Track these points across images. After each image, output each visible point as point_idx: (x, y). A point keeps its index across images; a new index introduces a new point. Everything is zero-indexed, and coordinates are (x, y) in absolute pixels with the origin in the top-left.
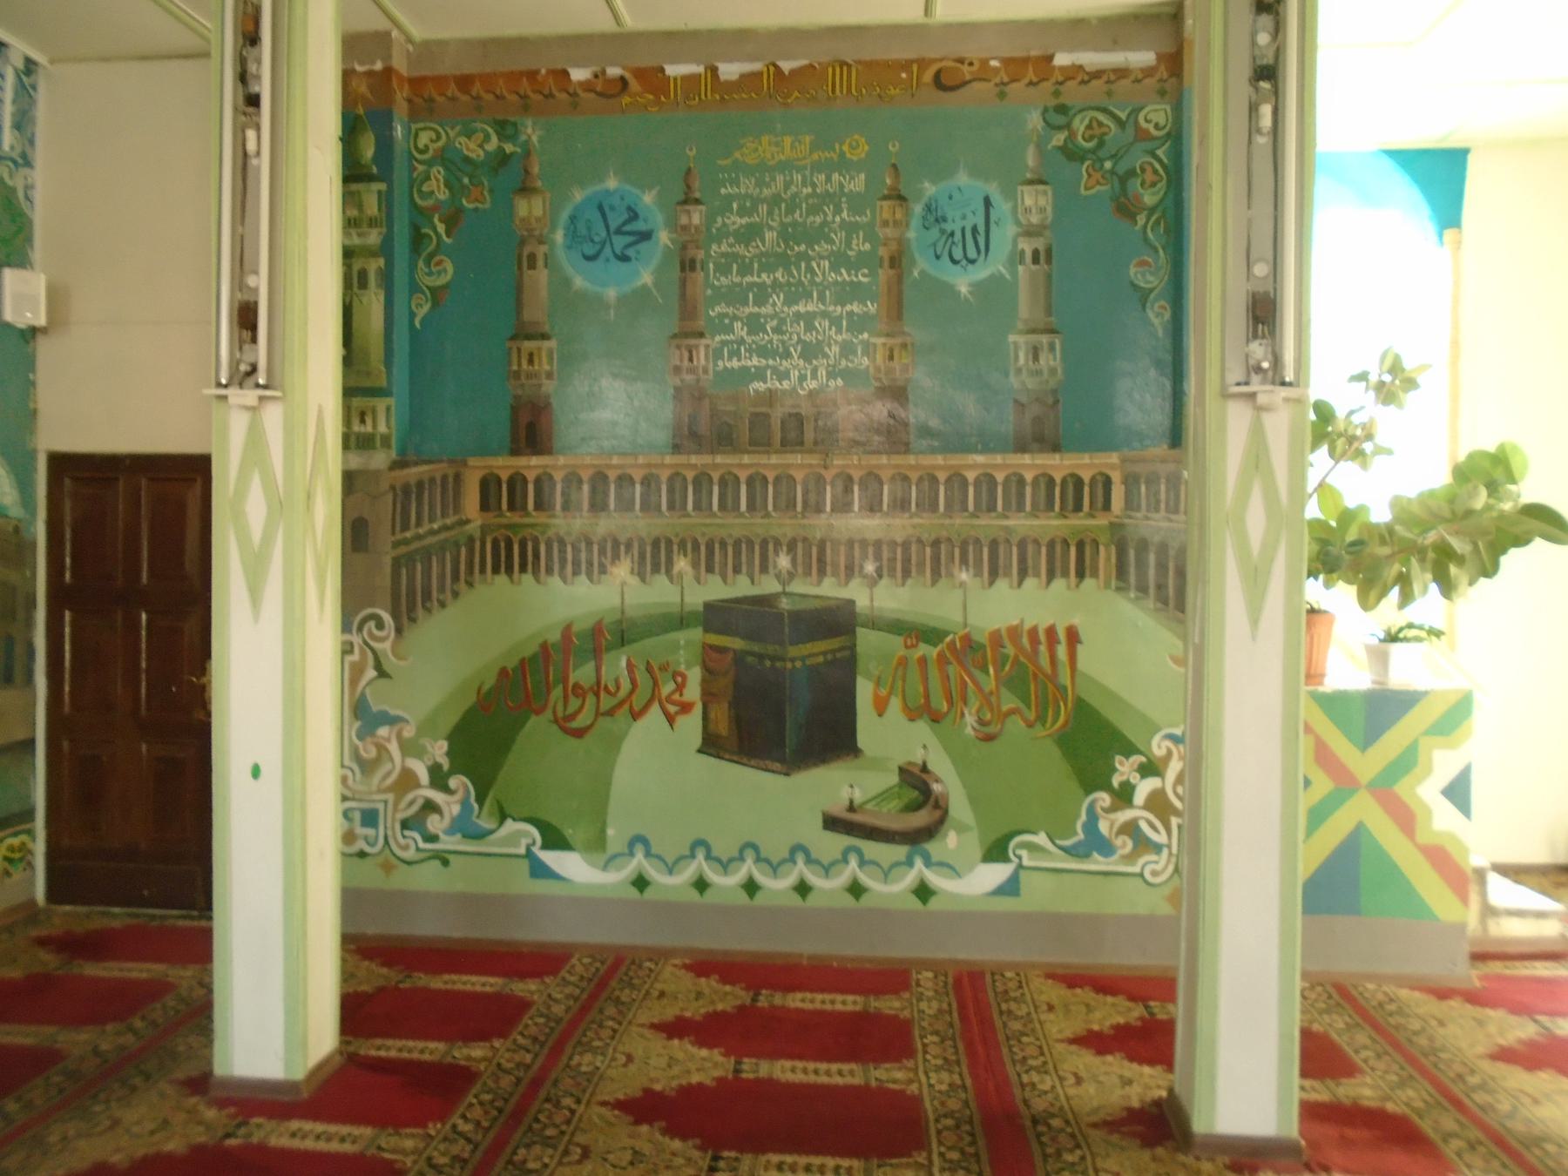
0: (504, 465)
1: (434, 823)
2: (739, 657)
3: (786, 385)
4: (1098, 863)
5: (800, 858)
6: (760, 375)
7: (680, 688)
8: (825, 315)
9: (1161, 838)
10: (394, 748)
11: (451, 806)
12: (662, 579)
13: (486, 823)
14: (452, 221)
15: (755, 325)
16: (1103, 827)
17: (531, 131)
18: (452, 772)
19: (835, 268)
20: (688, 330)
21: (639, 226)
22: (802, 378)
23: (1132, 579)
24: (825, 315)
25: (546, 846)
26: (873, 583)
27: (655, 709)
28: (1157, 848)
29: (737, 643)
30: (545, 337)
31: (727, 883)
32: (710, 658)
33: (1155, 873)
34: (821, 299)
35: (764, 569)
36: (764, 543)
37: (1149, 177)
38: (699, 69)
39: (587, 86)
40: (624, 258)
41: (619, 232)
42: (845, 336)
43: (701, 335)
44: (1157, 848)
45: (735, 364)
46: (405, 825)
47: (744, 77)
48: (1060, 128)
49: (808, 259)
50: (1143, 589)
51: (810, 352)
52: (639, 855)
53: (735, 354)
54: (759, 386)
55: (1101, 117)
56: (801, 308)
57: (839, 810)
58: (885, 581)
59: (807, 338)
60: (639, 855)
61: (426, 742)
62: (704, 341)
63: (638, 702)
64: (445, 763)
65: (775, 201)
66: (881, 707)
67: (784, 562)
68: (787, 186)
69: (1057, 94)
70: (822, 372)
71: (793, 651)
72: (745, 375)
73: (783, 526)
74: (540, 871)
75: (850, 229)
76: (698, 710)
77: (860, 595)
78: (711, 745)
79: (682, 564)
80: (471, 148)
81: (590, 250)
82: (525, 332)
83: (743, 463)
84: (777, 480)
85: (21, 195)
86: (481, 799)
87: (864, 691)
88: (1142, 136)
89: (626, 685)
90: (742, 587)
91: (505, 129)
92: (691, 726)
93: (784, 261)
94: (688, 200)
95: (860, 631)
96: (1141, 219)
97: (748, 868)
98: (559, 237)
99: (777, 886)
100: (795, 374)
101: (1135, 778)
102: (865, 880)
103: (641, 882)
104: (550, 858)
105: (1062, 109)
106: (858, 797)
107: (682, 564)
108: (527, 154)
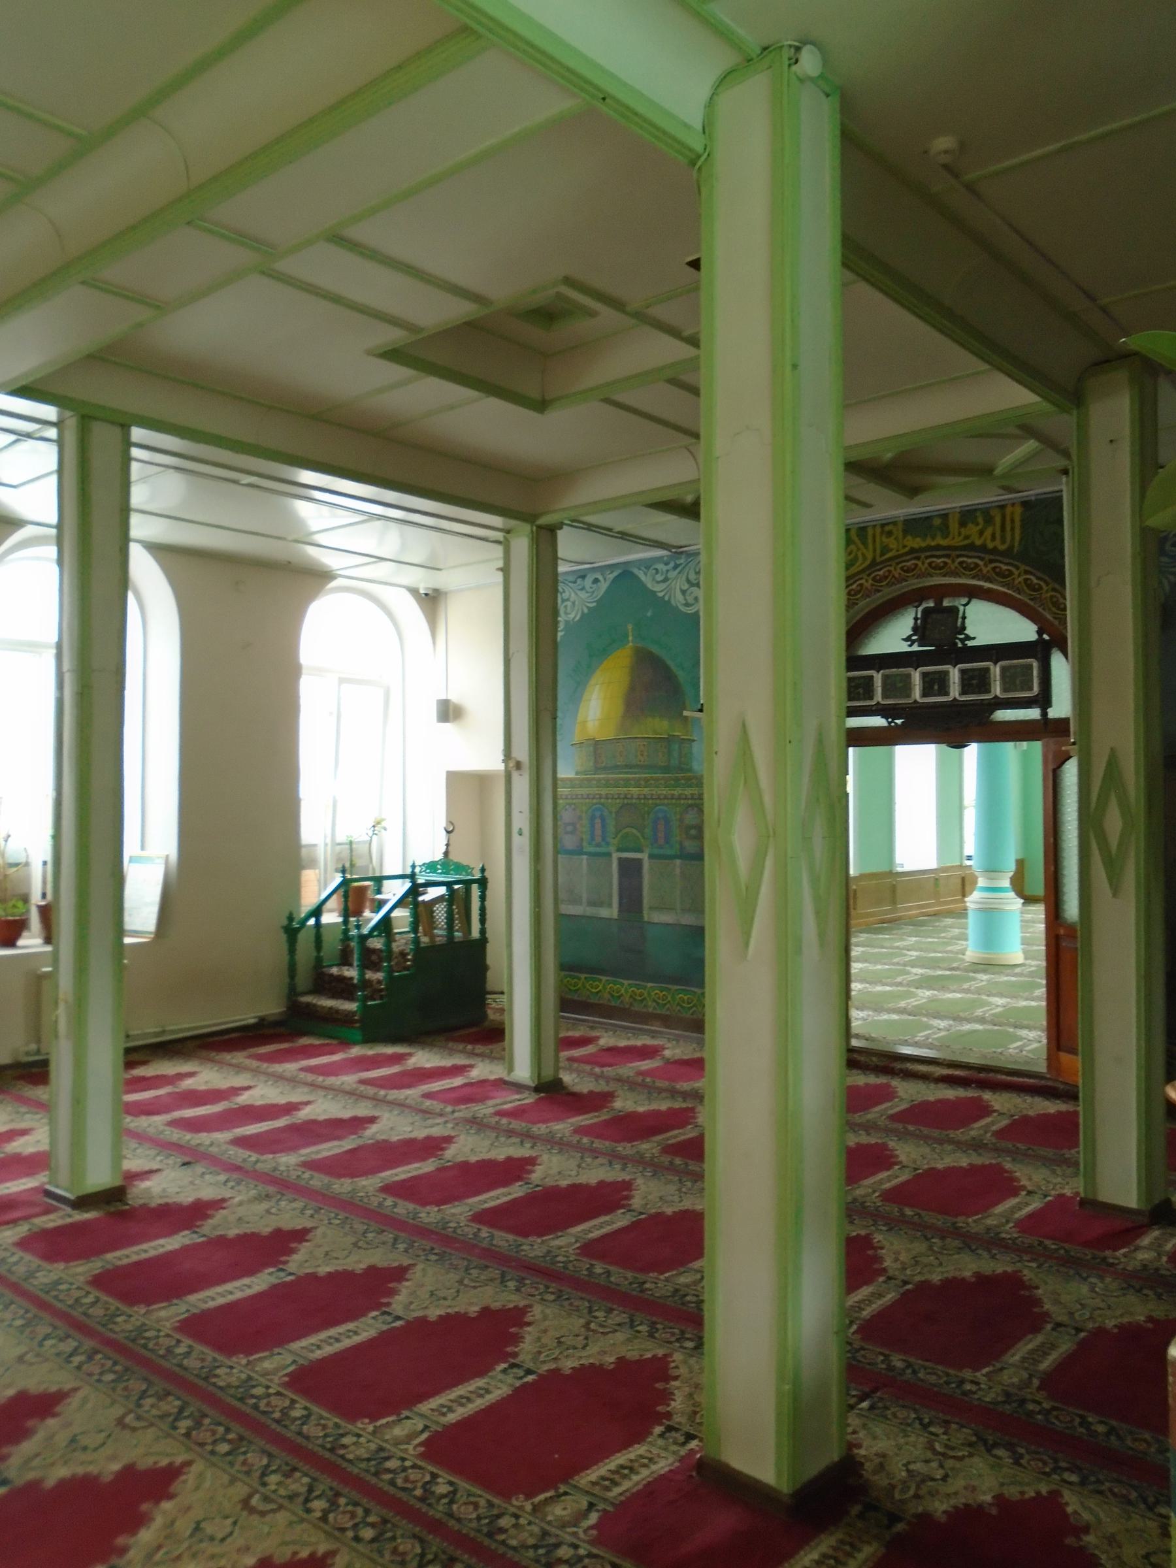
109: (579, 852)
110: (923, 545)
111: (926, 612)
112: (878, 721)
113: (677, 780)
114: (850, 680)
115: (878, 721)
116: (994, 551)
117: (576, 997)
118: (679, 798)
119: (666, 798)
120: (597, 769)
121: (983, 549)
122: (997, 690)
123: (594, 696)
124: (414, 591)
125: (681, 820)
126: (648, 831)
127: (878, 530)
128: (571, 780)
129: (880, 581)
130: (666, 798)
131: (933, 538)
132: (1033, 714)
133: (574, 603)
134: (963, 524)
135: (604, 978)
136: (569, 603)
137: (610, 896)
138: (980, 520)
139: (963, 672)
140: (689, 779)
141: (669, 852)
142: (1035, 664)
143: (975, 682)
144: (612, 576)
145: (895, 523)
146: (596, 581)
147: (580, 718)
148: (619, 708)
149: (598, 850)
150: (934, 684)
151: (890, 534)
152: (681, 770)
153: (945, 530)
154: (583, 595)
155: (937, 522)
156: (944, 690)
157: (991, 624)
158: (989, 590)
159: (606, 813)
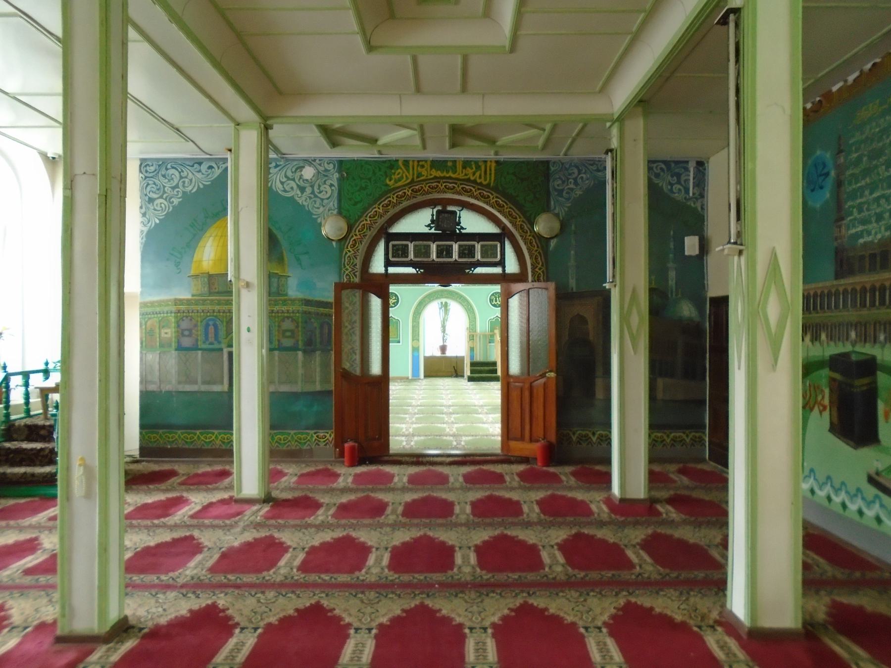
15: (860, 211)
21: (825, 171)
22: (876, 233)
35: (847, 339)
41: (821, 175)
43: (842, 219)
45: (853, 231)
53: (854, 226)
54: (861, 241)
62: (844, 222)
68: (871, 129)
70: (883, 228)
72: (859, 235)
84: (852, 289)
85: (699, 209)
87: (881, 407)
93: (867, 172)
94: (840, 152)
95: (879, 373)
106: (880, 466)
109: (195, 348)
110: (442, 175)
111: (438, 212)
112: (410, 270)
113: (276, 301)
115: (410, 270)
116: (481, 184)
117: (191, 447)
118: (278, 312)
120: (211, 293)
121: (475, 182)
122: (478, 256)
124: (44, 156)
125: (279, 326)
127: (416, 163)
128: (188, 300)
129: (416, 192)
131: (448, 172)
132: (498, 270)
133: (191, 180)
134: (464, 167)
135: (216, 432)
136: (186, 180)
137: (223, 377)
138: (474, 166)
139: (460, 246)
140: (285, 300)
142: (499, 245)
143: (467, 252)
145: (426, 161)
146: (211, 167)
149: (211, 346)
150: (445, 251)
151: (423, 166)
153: (454, 168)
154: (199, 175)
155: (450, 164)
156: (449, 254)
157: (472, 223)
158: (472, 205)
159: (218, 323)
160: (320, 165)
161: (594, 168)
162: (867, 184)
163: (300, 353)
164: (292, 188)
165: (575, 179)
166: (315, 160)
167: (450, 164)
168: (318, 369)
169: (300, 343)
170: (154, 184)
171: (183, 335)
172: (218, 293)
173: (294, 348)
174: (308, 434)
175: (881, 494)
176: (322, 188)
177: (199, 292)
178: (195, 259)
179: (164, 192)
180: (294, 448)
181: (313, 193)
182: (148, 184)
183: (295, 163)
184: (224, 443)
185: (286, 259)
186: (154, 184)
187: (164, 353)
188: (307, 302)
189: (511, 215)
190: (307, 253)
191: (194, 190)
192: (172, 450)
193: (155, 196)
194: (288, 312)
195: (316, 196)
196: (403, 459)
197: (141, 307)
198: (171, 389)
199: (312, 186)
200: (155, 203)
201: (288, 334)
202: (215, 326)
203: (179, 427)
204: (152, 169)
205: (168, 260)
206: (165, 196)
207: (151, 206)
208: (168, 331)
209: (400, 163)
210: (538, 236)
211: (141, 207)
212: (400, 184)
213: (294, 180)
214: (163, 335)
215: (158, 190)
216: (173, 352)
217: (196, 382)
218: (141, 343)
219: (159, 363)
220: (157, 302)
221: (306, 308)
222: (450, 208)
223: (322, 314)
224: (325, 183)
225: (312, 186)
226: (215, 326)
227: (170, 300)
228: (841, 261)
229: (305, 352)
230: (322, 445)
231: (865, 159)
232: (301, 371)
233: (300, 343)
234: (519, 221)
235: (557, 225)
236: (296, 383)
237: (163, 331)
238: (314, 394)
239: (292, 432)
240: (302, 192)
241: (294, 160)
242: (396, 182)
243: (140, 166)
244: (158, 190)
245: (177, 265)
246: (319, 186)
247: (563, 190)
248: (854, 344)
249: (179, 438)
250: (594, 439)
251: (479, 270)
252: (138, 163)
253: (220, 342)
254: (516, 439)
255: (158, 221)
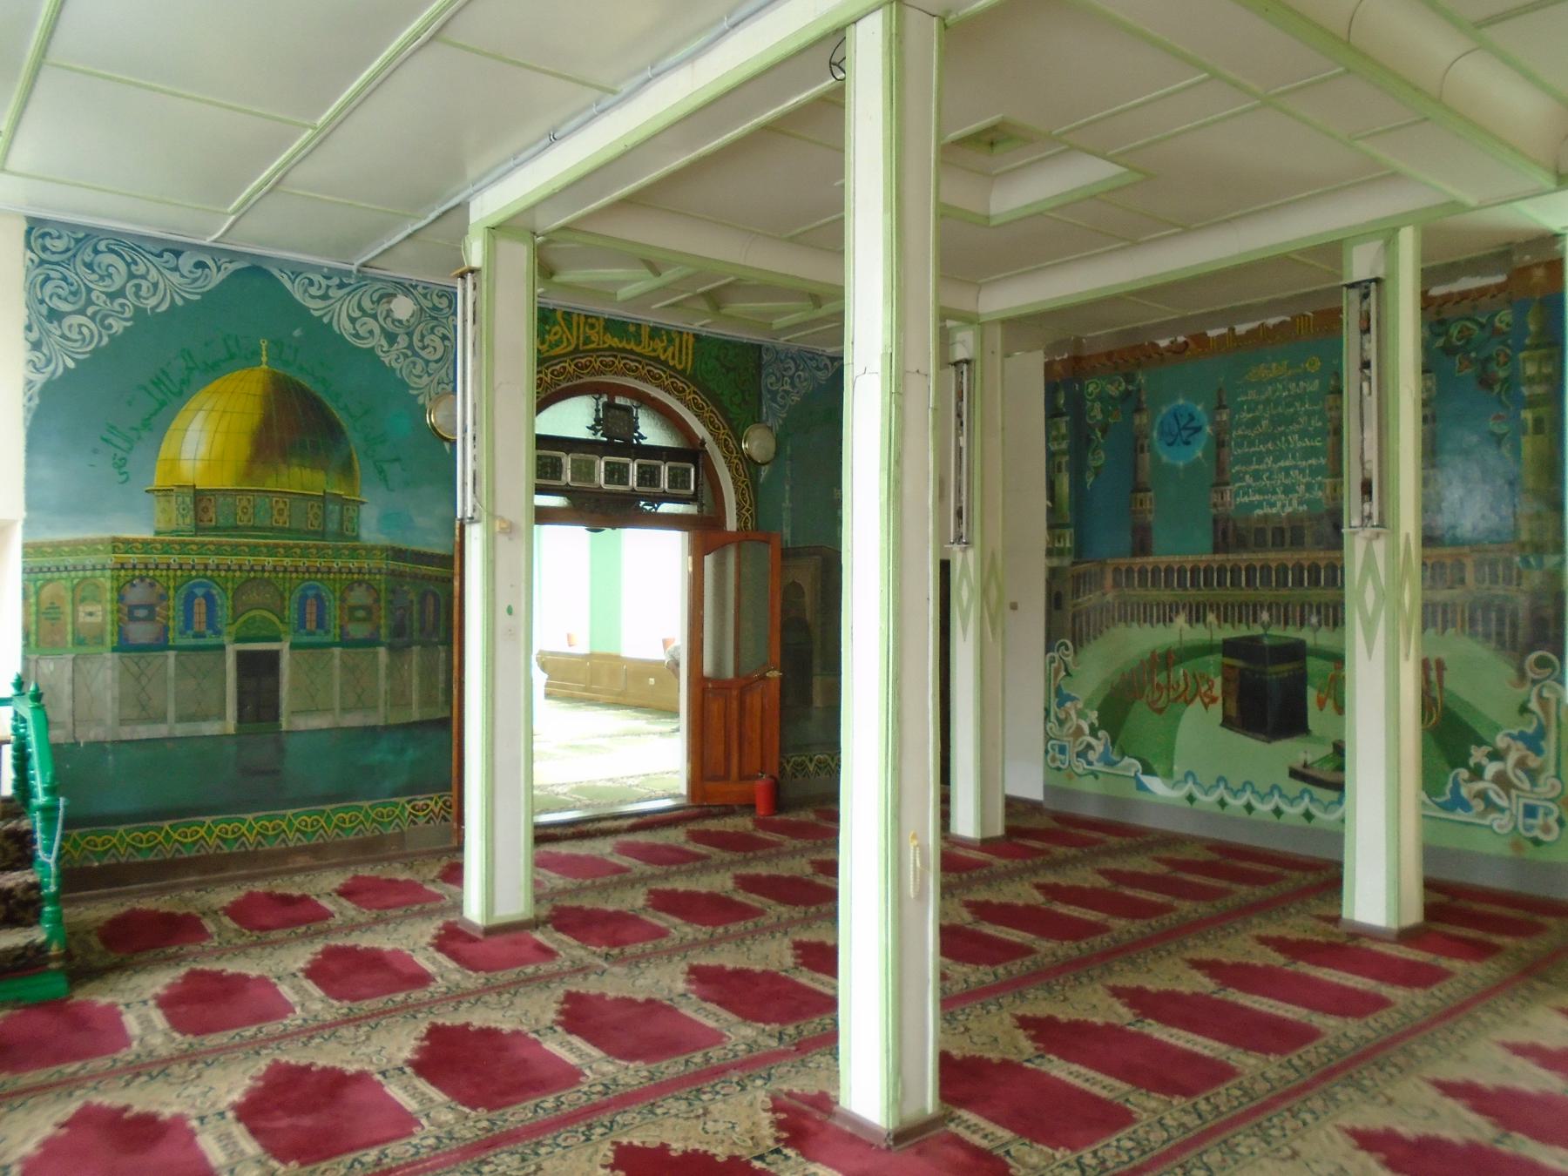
0: (1125, 562)
1: (1092, 756)
2: (1242, 671)
3: (1274, 511)
4: (1460, 815)
5: (1276, 794)
6: (1260, 505)
7: (1210, 688)
8: (1296, 467)
9: (1503, 803)
10: (1073, 714)
11: (1099, 746)
12: (1200, 626)
13: (1115, 758)
14: (1104, 432)
15: (1257, 476)
16: (1464, 792)
17: (1141, 378)
18: (1100, 728)
19: (1301, 439)
20: (1221, 483)
21: (1195, 424)
22: (1283, 506)
23: (1480, 629)
24: (1296, 467)
25: (1144, 773)
26: (1316, 629)
27: (1198, 699)
28: (1501, 810)
29: (1239, 663)
30: (1148, 490)
31: (1236, 803)
32: (1226, 671)
33: (1500, 827)
34: (1294, 457)
35: (1255, 621)
36: (1255, 606)
37: (1502, 359)
38: (1224, 331)
39: (1168, 349)
40: (1187, 443)
41: (1185, 428)
42: (1308, 479)
44: (1501, 810)
45: (1246, 499)
46: (1079, 755)
47: (1249, 332)
48: (1439, 335)
49: (1286, 435)
50: (1487, 636)
51: (1288, 490)
52: (1190, 784)
53: (1246, 494)
54: (1259, 512)
55: (1469, 324)
56: (1282, 464)
57: (1298, 766)
58: (1323, 628)
59: (1287, 482)
60: (1190, 784)
61: (1087, 711)
63: (1189, 695)
64: (1096, 723)
65: (1267, 402)
66: (1321, 704)
67: (1265, 616)
68: (1274, 392)
69: (1438, 313)
70: (1295, 502)
71: (1271, 669)
73: (1266, 595)
74: (1141, 787)
75: (1310, 414)
76: (1220, 701)
77: (1307, 636)
78: (1227, 722)
79: (1211, 617)
80: (1112, 390)
81: (1171, 440)
82: (1138, 488)
83: (1244, 558)
84: (1262, 568)
86: (1113, 743)
87: (1312, 695)
88: (1496, 332)
89: (1182, 683)
90: (1242, 631)
91: (1129, 378)
92: (1217, 710)
93: (1273, 438)
94: (1221, 407)
96: (1497, 388)
97: (1248, 796)
98: (1155, 434)
99: (1264, 808)
100: (1279, 504)
101: (1485, 761)
102: (1314, 810)
103: (1191, 798)
104: (1146, 779)
105: (1441, 322)
106: (1310, 759)
107: (1211, 617)
108: (1139, 390)
109: (161, 644)
114: (539, 458)
116: (673, 368)
117: (151, 857)
119: (318, 571)
120: (199, 529)
121: (665, 363)
123: (196, 425)
125: (343, 600)
126: (291, 613)
127: (582, 319)
128: (145, 543)
130: (318, 571)
131: (628, 342)
133: (155, 285)
134: (651, 338)
135: (208, 820)
140: (355, 549)
141: (329, 639)
144: (232, 267)
145: (597, 318)
146: (200, 265)
147: (166, 450)
148: (244, 448)
149: (201, 642)
151: (592, 326)
152: (341, 535)
154: (175, 278)
155: (632, 329)
156: (623, 480)
157: (651, 432)
158: (654, 399)
159: (215, 591)
160: (425, 296)
161: (814, 364)
162: (1269, 452)
163: (382, 651)
164: (371, 332)
165: (792, 378)
166: (415, 287)
167: (632, 329)
168: (415, 681)
169: (383, 631)
170: (65, 279)
171: (133, 619)
172: (216, 528)
173: (371, 642)
174: (396, 805)
175: (1310, 787)
176: (427, 341)
177: (174, 527)
178: (162, 455)
179: (90, 302)
180: (368, 834)
181: (410, 346)
182: (48, 279)
183: (379, 285)
184: (224, 840)
185: (357, 466)
186: (65, 279)
187: (86, 657)
188: (399, 554)
189: (712, 423)
190: (398, 460)
191: (163, 308)
192: (103, 870)
193: (64, 307)
194: (360, 571)
195: (415, 354)
196: (558, 831)
197: (25, 555)
198: (101, 737)
199: (410, 335)
200: (67, 322)
201: (361, 614)
202: (209, 598)
203: (119, 819)
204: (60, 245)
205: (95, 451)
206: (90, 311)
207: (53, 327)
208: (97, 608)
209: (559, 315)
210: (749, 460)
211: (29, 328)
212: (557, 351)
213: (375, 317)
214: (82, 618)
215: (74, 294)
216: (109, 655)
217: (162, 719)
218: (26, 635)
219: (73, 681)
220: (67, 543)
221: (393, 565)
222: (619, 401)
223: (423, 577)
224: (432, 332)
225: (410, 335)
226: (209, 598)
227: (102, 541)
228: (1225, 533)
229: (392, 648)
230: (421, 822)
231: (1264, 423)
232: (383, 685)
233: (383, 631)
234: (723, 433)
235: (771, 445)
236: (375, 708)
237: (83, 609)
238: (408, 726)
239: (366, 804)
240: (391, 345)
241: (375, 279)
242: (551, 347)
243: (29, 232)
244: (74, 294)
245: (120, 464)
246: (423, 337)
247: (776, 392)
248: (1266, 627)
249: (122, 842)
250: (811, 767)
251: (665, 508)
252: (24, 226)
253: (218, 633)
254: (715, 779)
255: (71, 364)
